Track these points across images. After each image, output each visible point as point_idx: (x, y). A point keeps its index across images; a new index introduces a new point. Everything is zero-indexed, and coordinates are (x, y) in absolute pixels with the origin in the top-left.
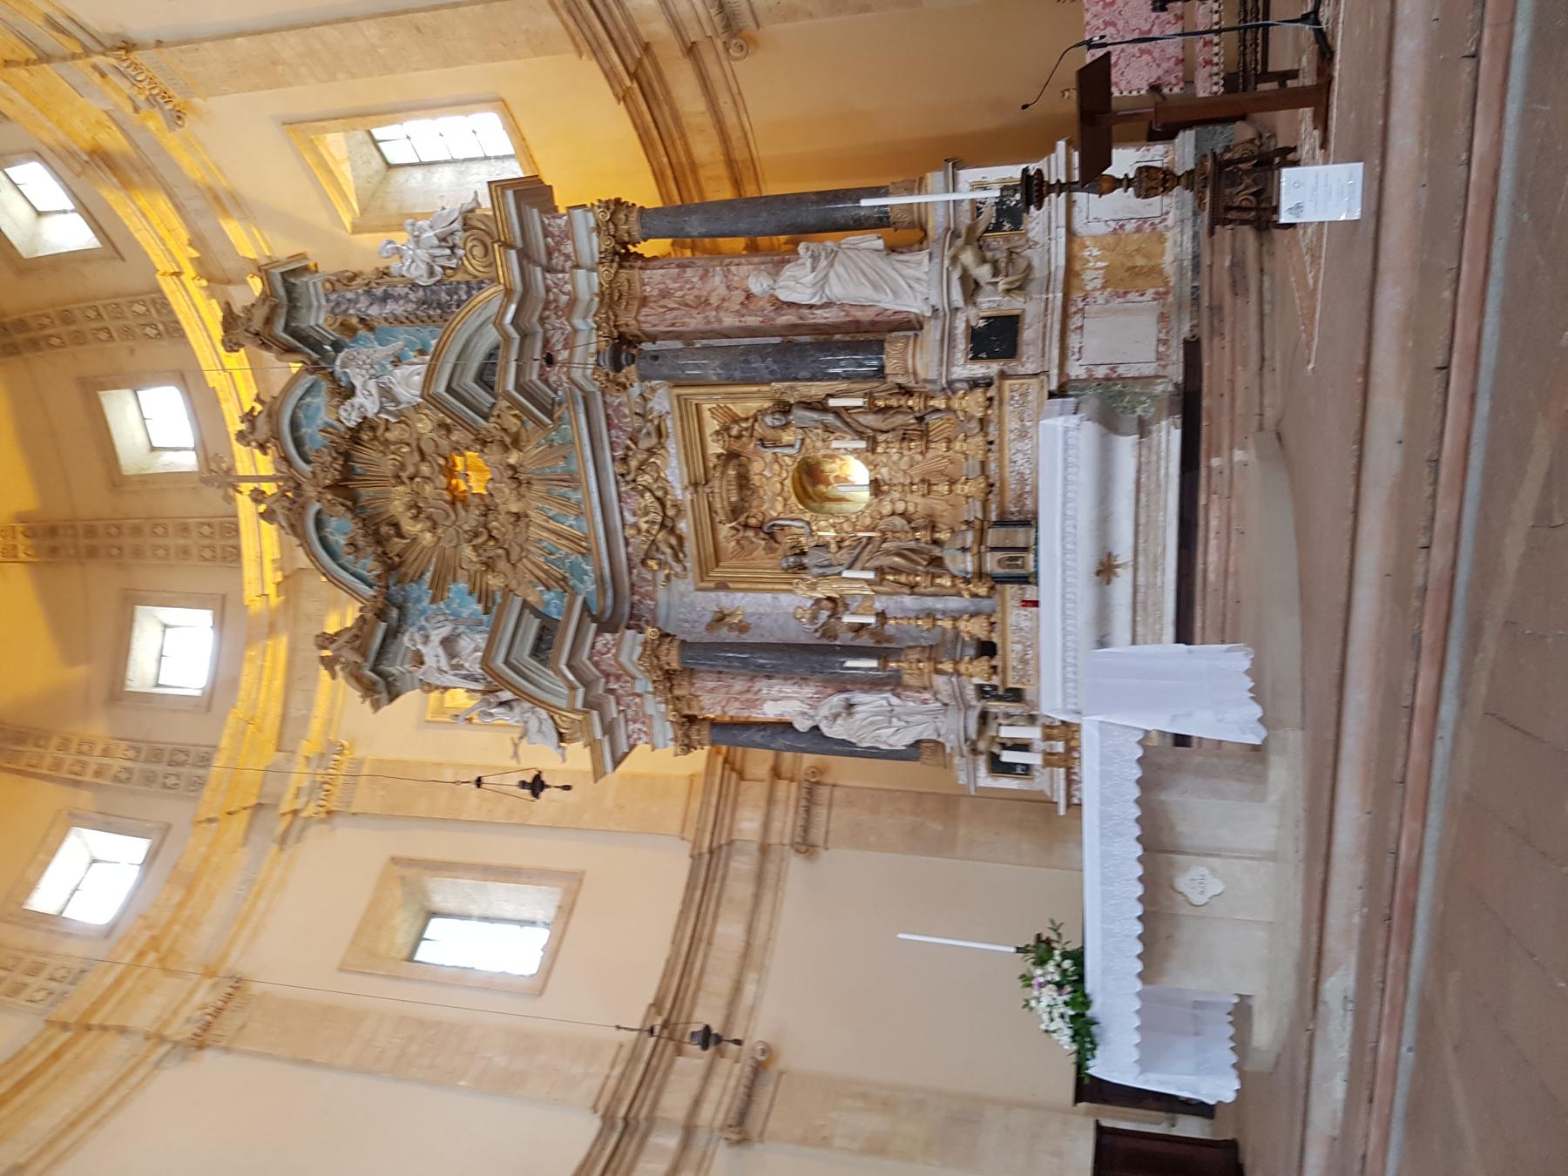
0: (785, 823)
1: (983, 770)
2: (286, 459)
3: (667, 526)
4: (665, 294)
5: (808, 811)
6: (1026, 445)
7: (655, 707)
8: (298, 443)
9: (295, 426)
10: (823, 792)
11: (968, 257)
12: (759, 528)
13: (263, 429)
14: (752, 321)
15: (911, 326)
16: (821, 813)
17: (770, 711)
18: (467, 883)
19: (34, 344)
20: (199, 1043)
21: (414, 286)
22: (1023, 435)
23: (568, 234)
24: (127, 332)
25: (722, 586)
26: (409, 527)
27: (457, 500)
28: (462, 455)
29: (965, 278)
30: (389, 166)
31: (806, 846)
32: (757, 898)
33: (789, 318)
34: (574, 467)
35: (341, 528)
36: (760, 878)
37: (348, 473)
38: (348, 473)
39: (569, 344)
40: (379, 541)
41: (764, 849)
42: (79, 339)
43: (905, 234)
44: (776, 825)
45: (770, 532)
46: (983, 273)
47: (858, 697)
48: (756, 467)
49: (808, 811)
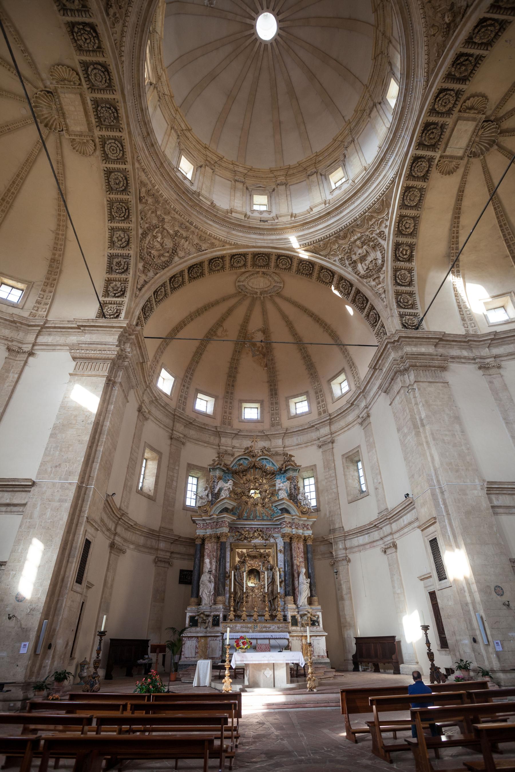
0: (161, 554)
1: (191, 614)
2: (260, 456)
3: (246, 538)
4: (299, 548)
5: (164, 561)
6: (276, 629)
7: (209, 532)
8: (263, 459)
9: (266, 459)
10: (167, 565)
11: (309, 615)
12: (244, 560)
13: (266, 452)
14: (295, 567)
15: (295, 602)
16: (163, 565)
17: (207, 561)
18: (155, 471)
19: (272, 395)
20: (140, 410)
21: (297, 495)
22: (278, 628)
23: (308, 529)
24: (273, 414)
25: (232, 550)
26: (244, 478)
27: (249, 490)
28: (260, 493)
29: (306, 614)
30: (304, 479)
31: (157, 561)
32: (147, 548)
33: (296, 575)
34: (258, 518)
35: (245, 463)
36: (152, 548)
37: (256, 468)
38: (256, 468)
39: (290, 527)
40: (243, 472)
41: (157, 549)
42: (272, 404)
43: (310, 602)
44: (162, 553)
45: (243, 562)
46: (305, 618)
47: (213, 585)
48: (257, 560)
49: (164, 561)
